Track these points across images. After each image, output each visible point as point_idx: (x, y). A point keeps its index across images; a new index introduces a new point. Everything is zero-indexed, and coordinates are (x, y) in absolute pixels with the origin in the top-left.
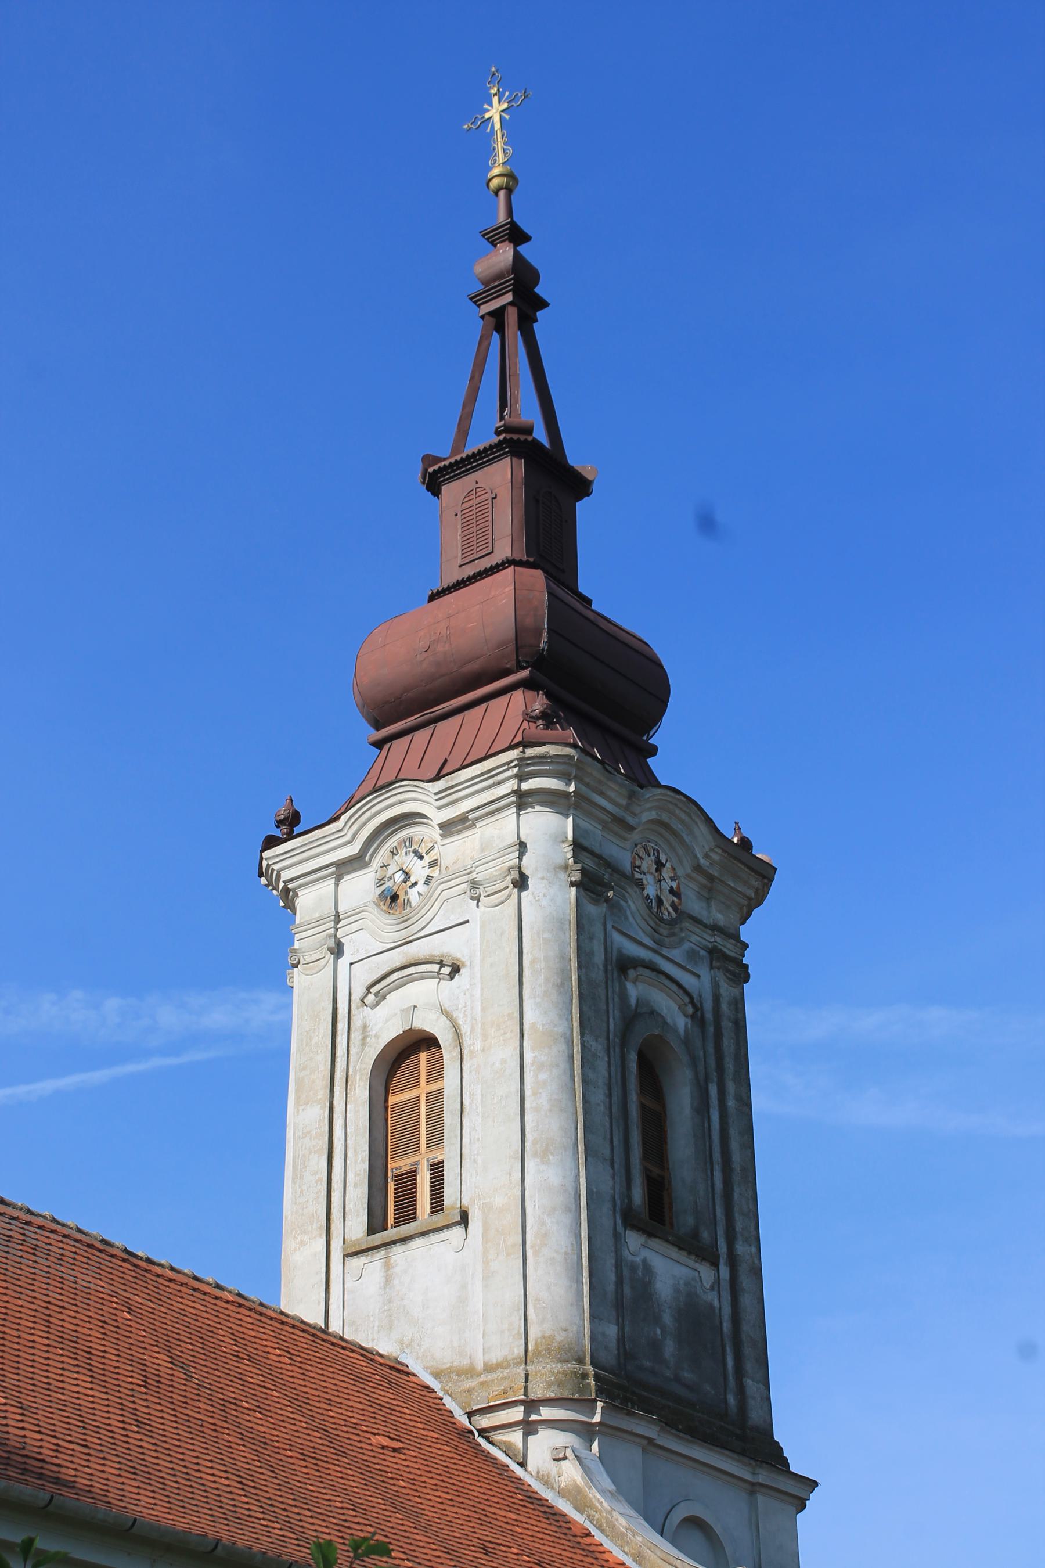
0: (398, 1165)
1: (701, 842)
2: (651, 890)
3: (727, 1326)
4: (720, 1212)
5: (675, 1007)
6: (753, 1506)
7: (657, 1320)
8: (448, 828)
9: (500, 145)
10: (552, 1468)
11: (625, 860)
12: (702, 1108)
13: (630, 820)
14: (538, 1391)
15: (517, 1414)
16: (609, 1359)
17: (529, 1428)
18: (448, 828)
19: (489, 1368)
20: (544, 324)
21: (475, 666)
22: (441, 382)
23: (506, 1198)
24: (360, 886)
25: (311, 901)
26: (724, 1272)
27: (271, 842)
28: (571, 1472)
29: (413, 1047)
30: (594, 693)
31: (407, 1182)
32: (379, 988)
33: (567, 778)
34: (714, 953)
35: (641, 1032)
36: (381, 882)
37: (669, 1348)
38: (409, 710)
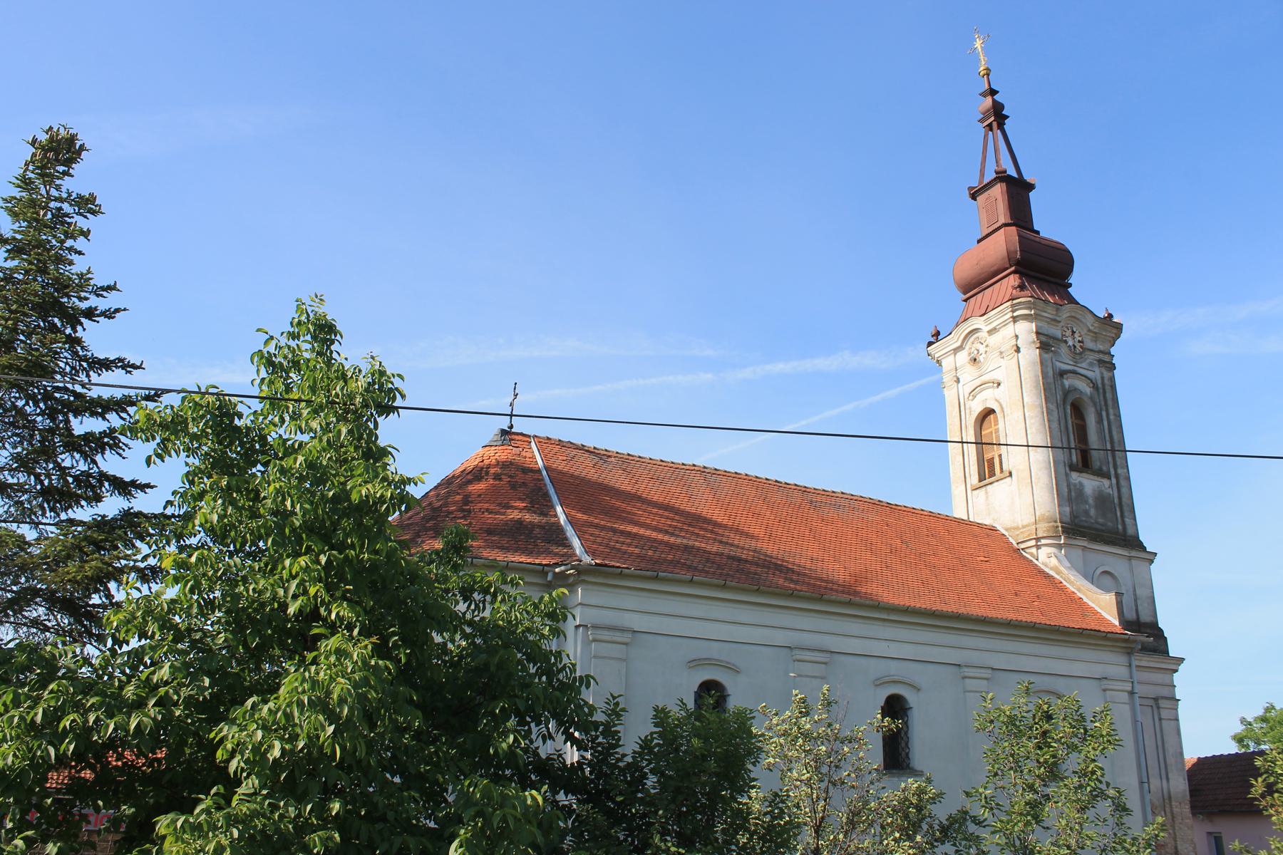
0: (987, 456)
1: (1089, 321)
2: (1070, 343)
3: (1116, 501)
6: (1130, 564)
7: (1086, 502)
8: (991, 332)
10: (1047, 560)
11: (1058, 334)
12: (1100, 421)
14: (1040, 535)
15: (1033, 543)
16: (1067, 519)
17: (1038, 547)
18: (991, 332)
19: (1024, 527)
20: (1008, 125)
22: (970, 156)
23: (1025, 466)
24: (963, 357)
25: (947, 363)
26: (1114, 481)
27: (930, 344)
28: (1054, 561)
29: (989, 412)
30: (1043, 268)
31: (991, 461)
32: (973, 393)
33: (1030, 309)
34: (1100, 362)
35: (1070, 399)
37: (1092, 512)
38: (973, 286)
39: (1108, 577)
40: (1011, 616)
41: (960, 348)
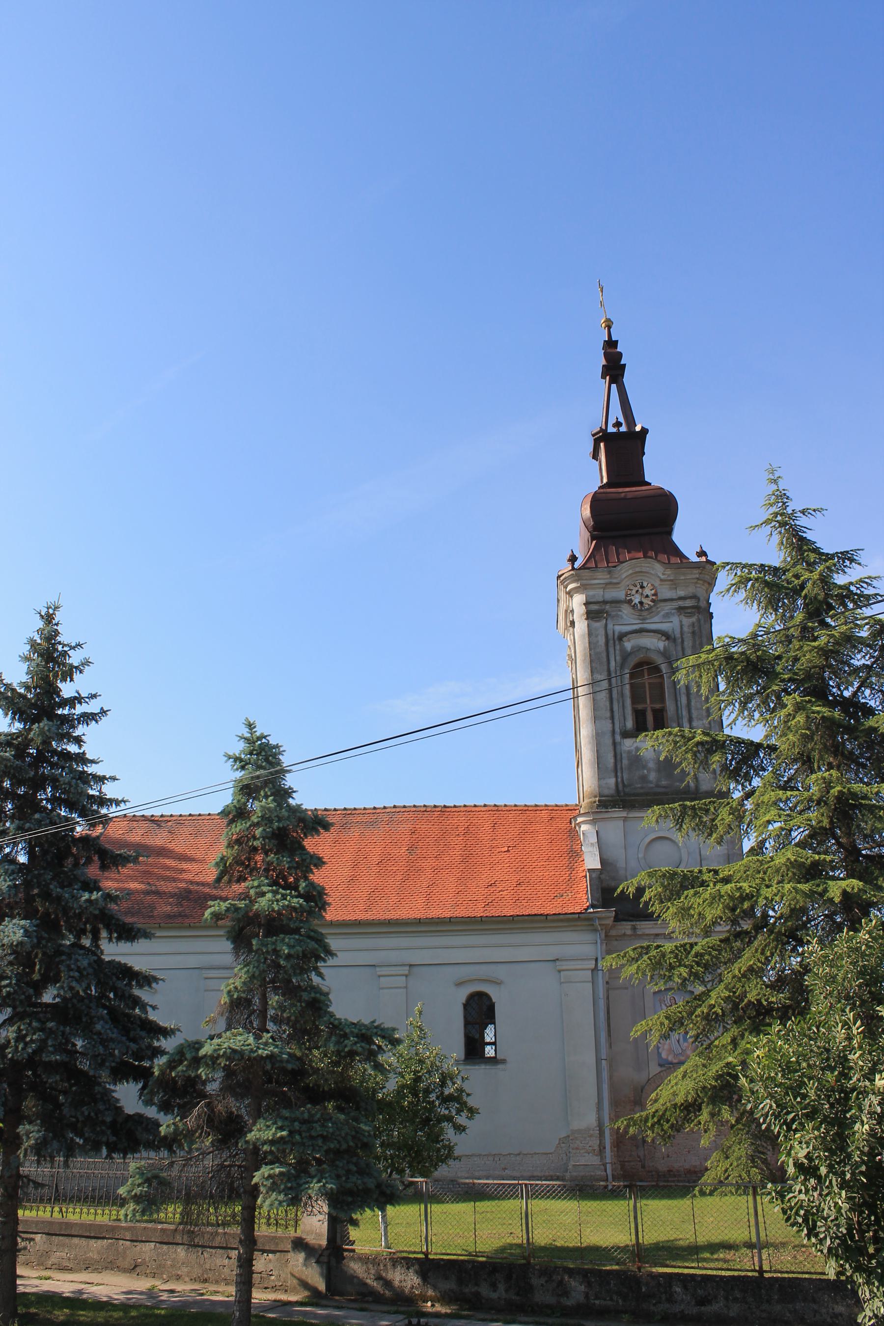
2: (636, 600)
4: (685, 713)
5: (655, 641)
7: (644, 767)
11: (620, 594)
13: (615, 581)
37: (653, 776)
39: (668, 842)
40: (461, 912)
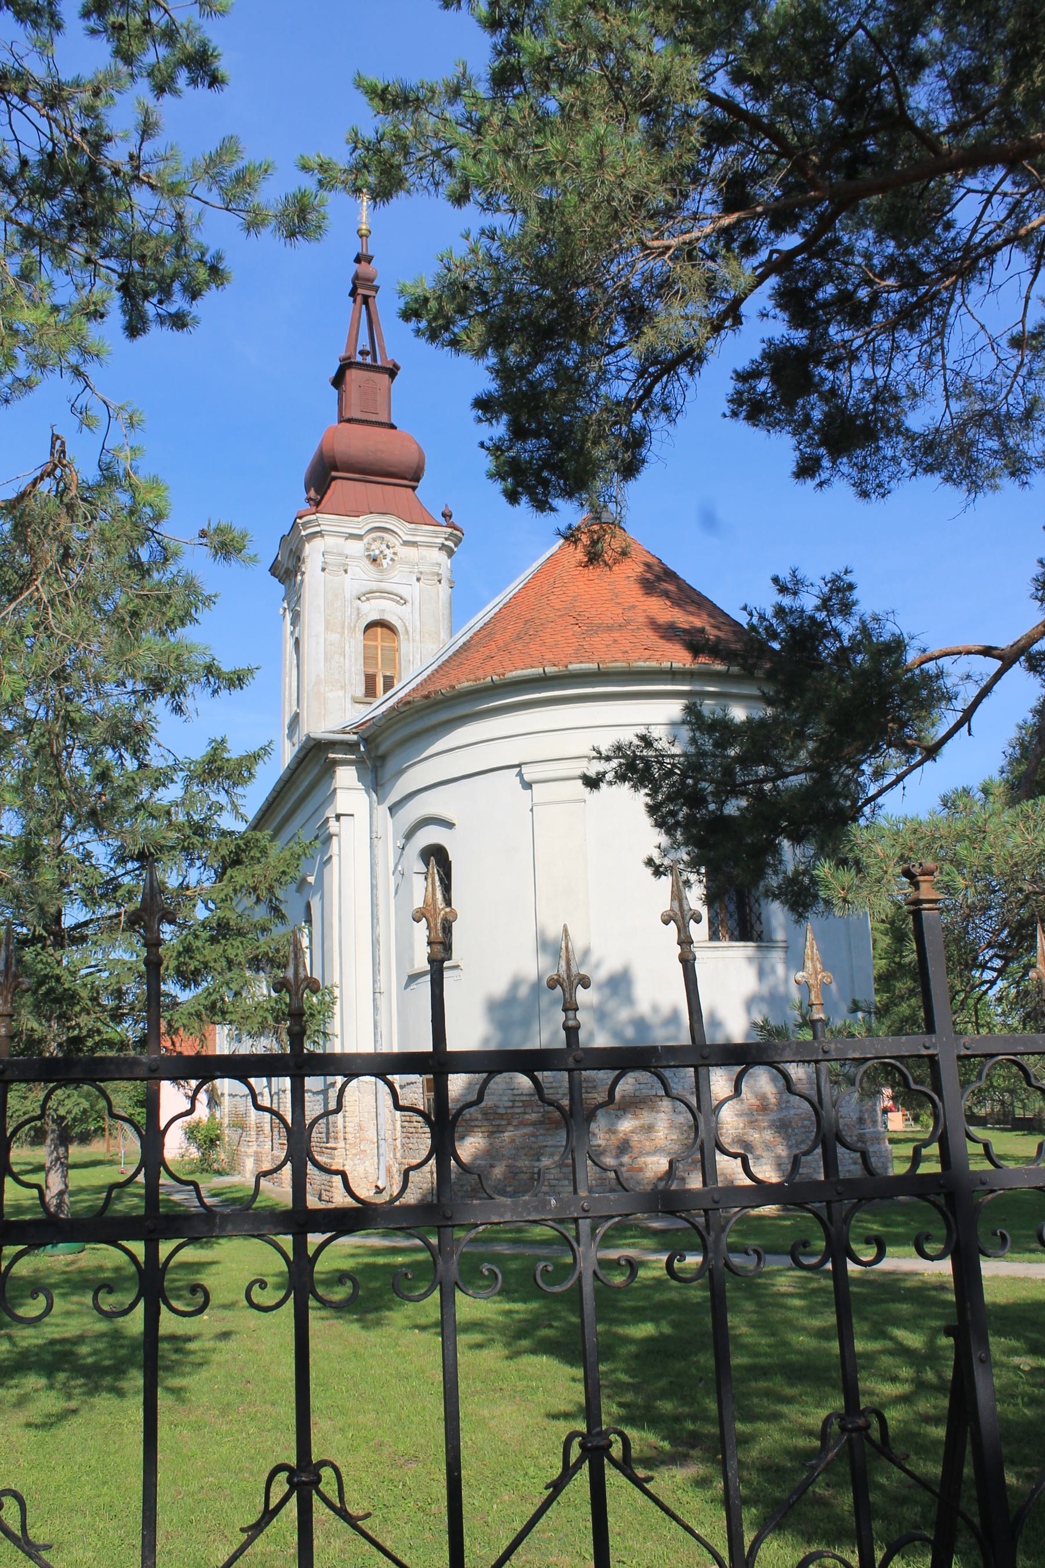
8: (406, 543)
9: (364, 214)
18: (406, 543)
21: (393, 470)
24: (356, 548)
36: (368, 549)
41: (359, 537)
